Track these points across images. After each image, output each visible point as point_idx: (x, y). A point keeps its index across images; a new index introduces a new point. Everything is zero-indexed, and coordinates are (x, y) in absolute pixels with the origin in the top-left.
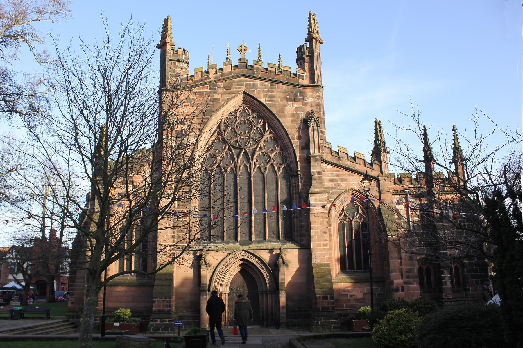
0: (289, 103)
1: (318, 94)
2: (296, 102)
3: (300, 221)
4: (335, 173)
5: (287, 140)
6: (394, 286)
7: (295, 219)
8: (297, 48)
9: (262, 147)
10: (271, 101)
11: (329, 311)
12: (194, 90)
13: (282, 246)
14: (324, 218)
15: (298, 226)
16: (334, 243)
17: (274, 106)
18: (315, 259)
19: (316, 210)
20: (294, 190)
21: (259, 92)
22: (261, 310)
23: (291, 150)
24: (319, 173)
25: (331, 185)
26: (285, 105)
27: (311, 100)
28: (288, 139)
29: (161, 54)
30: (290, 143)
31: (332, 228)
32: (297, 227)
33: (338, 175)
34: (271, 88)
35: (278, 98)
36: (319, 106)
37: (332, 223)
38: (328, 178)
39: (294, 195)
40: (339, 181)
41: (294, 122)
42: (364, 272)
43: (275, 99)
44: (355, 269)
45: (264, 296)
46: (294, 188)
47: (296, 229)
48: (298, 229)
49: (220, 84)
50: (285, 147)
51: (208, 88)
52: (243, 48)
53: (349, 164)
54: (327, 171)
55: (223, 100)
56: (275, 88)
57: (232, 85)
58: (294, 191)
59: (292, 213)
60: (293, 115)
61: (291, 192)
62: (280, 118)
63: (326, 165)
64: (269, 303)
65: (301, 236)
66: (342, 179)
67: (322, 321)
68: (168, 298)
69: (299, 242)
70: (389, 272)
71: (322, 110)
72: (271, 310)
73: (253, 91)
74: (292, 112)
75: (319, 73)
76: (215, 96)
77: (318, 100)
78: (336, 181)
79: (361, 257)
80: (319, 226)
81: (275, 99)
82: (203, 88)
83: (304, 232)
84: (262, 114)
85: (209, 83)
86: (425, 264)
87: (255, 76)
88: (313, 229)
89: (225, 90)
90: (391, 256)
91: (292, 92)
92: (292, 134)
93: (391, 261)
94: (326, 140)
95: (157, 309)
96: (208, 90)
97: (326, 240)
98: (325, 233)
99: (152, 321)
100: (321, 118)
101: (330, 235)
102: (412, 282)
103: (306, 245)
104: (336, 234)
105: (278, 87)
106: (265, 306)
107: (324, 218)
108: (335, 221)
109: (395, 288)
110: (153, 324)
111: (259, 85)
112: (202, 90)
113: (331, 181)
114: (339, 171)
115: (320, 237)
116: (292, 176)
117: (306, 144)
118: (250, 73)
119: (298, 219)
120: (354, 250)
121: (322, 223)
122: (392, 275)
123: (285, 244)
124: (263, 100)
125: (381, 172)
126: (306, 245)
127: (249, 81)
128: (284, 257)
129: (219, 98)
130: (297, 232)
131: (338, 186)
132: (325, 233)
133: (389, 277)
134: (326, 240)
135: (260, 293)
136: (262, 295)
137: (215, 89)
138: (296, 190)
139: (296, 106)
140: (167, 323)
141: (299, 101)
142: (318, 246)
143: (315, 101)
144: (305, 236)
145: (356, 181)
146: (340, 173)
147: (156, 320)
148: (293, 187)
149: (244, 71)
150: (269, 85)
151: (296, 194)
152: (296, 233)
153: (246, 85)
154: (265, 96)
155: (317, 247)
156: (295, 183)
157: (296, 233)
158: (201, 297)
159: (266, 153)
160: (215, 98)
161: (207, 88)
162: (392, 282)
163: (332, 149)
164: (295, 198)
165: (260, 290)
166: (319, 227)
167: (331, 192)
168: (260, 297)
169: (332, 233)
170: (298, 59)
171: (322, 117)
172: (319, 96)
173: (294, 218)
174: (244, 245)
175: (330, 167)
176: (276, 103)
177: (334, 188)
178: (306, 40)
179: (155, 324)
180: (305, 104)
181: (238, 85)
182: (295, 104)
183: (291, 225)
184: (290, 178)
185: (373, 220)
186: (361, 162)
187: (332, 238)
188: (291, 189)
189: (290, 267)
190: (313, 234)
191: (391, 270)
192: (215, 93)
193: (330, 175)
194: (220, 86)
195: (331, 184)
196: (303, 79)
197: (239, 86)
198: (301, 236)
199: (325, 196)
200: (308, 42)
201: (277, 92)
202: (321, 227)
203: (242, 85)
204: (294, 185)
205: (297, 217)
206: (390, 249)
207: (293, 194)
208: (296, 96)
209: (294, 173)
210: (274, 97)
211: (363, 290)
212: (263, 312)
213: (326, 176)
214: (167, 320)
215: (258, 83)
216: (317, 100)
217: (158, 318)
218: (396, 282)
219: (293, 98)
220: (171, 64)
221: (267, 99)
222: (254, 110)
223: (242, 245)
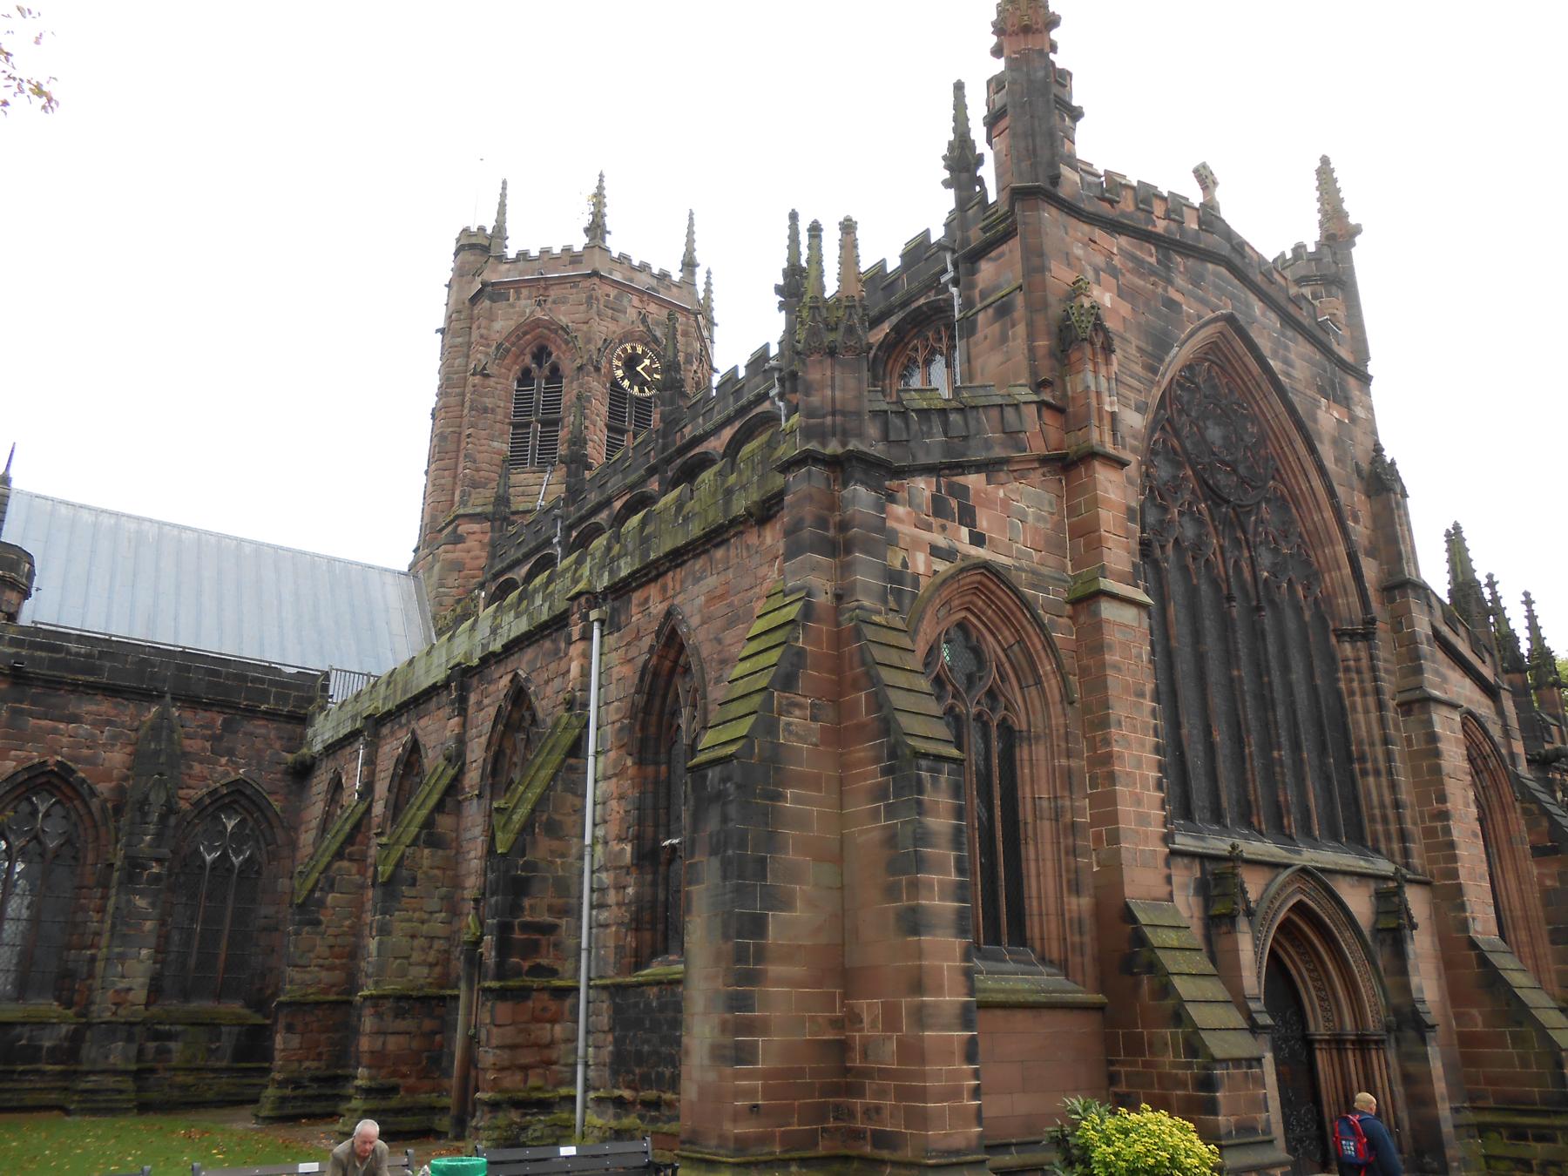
5: (1328, 514)
7: (1371, 779)
20: (1351, 680)
23: (1341, 549)
48: (1390, 813)
95: (1232, 1119)
119: (1384, 780)
135: (1320, 1041)
152: (1379, 828)
164: (1360, 708)
173: (1364, 773)
184: (1333, 640)
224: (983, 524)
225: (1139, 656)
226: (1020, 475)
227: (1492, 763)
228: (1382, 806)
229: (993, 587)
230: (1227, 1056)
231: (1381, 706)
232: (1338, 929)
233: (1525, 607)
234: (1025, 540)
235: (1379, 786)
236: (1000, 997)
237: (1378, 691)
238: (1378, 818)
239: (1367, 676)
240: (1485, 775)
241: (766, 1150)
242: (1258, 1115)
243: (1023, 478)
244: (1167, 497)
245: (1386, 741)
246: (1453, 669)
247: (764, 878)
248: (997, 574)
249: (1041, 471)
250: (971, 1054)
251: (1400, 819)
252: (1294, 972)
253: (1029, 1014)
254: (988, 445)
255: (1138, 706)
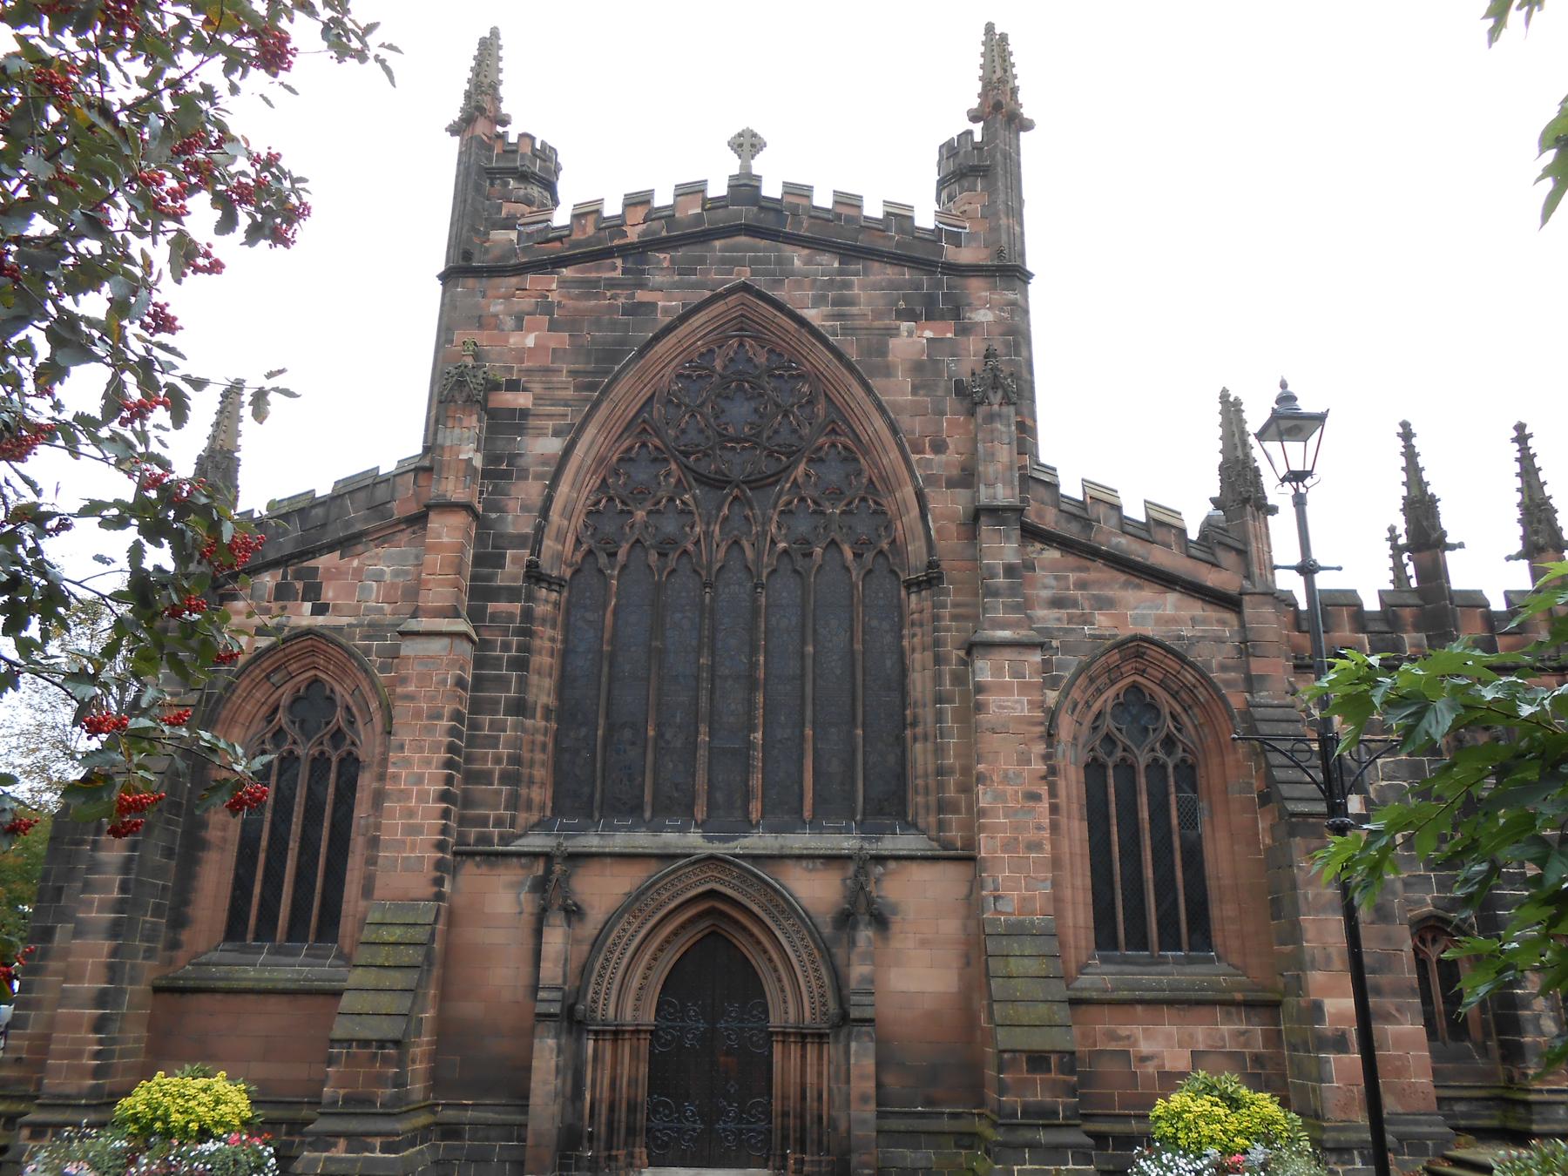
0: (905, 326)
1: (1010, 295)
2: (930, 323)
3: (939, 751)
4: (1072, 577)
5: (895, 454)
6: (1326, 1027)
7: (919, 746)
8: (941, 147)
9: (800, 480)
10: (840, 316)
11: (1056, 1122)
12: (566, 272)
13: (866, 846)
14: (1032, 740)
15: (931, 768)
16: (1070, 839)
17: (852, 335)
18: (996, 898)
19: (1001, 707)
20: (914, 635)
21: (798, 285)
22: (776, 1106)
23: (909, 491)
24: (1010, 570)
25: (1059, 619)
26: (893, 332)
27: (985, 315)
28: (898, 453)
29: (460, 153)
30: (903, 466)
31: (1062, 784)
32: (926, 775)
33: (1081, 585)
34: (841, 272)
35: (867, 309)
36: (1017, 335)
37: (1060, 762)
38: (1046, 594)
39: (917, 656)
40: (1086, 604)
41: (922, 392)
42: (1190, 961)
43: (854, 310)
44: (1156, 947)
45: (792, 1046)
46: (918, 630)
47: (920, 782)
48: (931, 781)
49: (662, 256)
50: (885, 480)
51: (615, 268)
52: (747, 142)
53: (1123, 543)
54: (1043, 568)
55: (666, 310)
56: (857, 274)
57: (702, 260)
58: (915, 640)
59: (908, 721)
60: (917, 368)
61: (905, 643)
62: (872, 376)
63: (1038, 546)
64: (811, 1077)
65: (942, 807)
66: (1097, 598)
67: (1027, 1167)
68: (388, 1045)
69: (933, 833)
70: (1299, 963)
71: (1024, 353)
72: (815, 1104)
73: (775, 281)
74: (915, 357)
75: (1017, 228)
76: (641, 296)
77: (1012, 318)
78: (1074, 603)
79: (1176, 900)
80: (1012, 768)
81: (854, 310)
82: (598, 270)
83: (951, 793)
84: (807, 364)
85: (624, 251)
86: (1434, 941)
87: (787, 230)
88: (988, 782)
89: (677, 278)
90: (1306, 898)
91: (919, 287)
92: (913, 432)
93: (1306, 919)
94: (1037, 457)
95: (342, 1092)
96: (617, 274)
97: (1039, 828)
98: (1034, 797)
99: (314, 1147)
100: (1019, 378)
101: (1054, 809)
102: (1394, 1012)
103: (959, 844)
104: (1075, 806)
105: (866, 273)
106: (792, 1089)
107: (1032, 740)
108: (1070, 754)
109: (1330, 1034)
110: (317, 1160)
111: (797, 262)
112: (594, 275)
113: (1057, 603)
114: (1087, 569)
115: (1015, 812)
116: (909, 585)
117: (963, 469)
118: (769, 221)
119: (930, 746)
120: (1149, 873)
121: (1025, 760)
122: (1316, 978)
123: (878, 840)
124: (812, 314)
125: (1248, 576)
126: (959, 844)
127: (765, 250)
128: (871, 887)
129: (654, 305)
130: (927, 793)
131: (1085, 623)
132: (1034, 797)
133: (1298, 986)
134: (1039, 828)
136: (783, 1042)
137: (643, 272)
138: (923, 635)
139: (928, 334)
140: (378, 1155)
141: (942, 318)
142: (1006, 847)
143: (997, 322)
144: (956, 811)
145: (1150, 608)
146: (1092, 576)
147: (332, 1140)
148: (913, 624)
149: (746, 214)
150: (836, 265)
151: (924, 650)
153: (754, 261)
154: (818, 301)
155: (1003, 852)
156: (921, 612)
157: (920, 799)
158: (536, 1041)
159: (815, 502)
160: (641, 304)
161: (616, 269)
162: (1317, 1008)
163: (1063, 490)
164: (918, 666)
165: (775, 1021)
166: (1011, 773)
167: (1055, 643)
168: (777, 1049)
169: (1062, 800)
170: (942, 184)
171: (1025, 375)
172: (1013, 304)
173: (915, 739)
174: (720, 840)
175: (1053, 554)
176: (858, 323)
177: (1067, 631)
178: (974, 117)
179: (327, 1159)
180: (964, 330)
181: (723, 261)
182: (923, 329)
183: (904, 767)
184: (903, 593)
185: (1223, 757)
186: (1172, 538)
187: (1063, 820)
188: (905, 632)
189: (895, 928)
190: (989, 797)
191: (1307, 958)
192: (642, 286)
193: (1053, 583)
194: (659, 262)
195: (1057, 615)
196: (958, 245)
197: (728, 263)
198: (942, 807)
199: (1036, 657)
200: (981, 124)
201: (863, 287)
202: (1018, 775)
203: (739, 262)
204: (916, 616)
205: (926, 738)
206: (1299, 867)
207: (913, 650)
208: (930, 301)
209: (917, 570)
210: (852, 303)
211: (1191, 1036)
212: (785, 1114)
213: (1044, 585)
214: (378, 1142)
215: (797, 258)
216: (1006, 315)
217: (338, 1135)
218: (1333, 1010)
219: (918, 309)
220: (492, 185)
221: (827, 309)
222: (778, 350)
223: (710, 840)
224: (328, 594)
225: (444, 682)
226: (383, 541)
227: (1202, 695)
228: (926, 775)
229: (324, 647)
230: (348, 1037)
231: (938, 660)
232: (769, 913)
233: (1516, 446)
234: (378, 597)
235: (925, 751)
236: (270, 986)
237: (937, 643)
238: (921, 790)
239: (928, 628)
240: (1196, 710)
241: (23, 1088)
242: (380, 1091)
243: (384, 542)
244: (629, 502)
245: (939, 699)
246: (1139, 587)
247: (59, 900)
248: (322, 636)
249: (410, 530)
250: (99, 1025)
251: (941, 787)
252: (753, 962)
253: (284, 999)
254: (348, 524)
255: (429, 730)
